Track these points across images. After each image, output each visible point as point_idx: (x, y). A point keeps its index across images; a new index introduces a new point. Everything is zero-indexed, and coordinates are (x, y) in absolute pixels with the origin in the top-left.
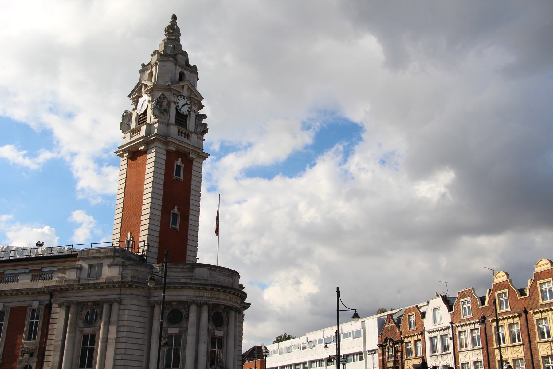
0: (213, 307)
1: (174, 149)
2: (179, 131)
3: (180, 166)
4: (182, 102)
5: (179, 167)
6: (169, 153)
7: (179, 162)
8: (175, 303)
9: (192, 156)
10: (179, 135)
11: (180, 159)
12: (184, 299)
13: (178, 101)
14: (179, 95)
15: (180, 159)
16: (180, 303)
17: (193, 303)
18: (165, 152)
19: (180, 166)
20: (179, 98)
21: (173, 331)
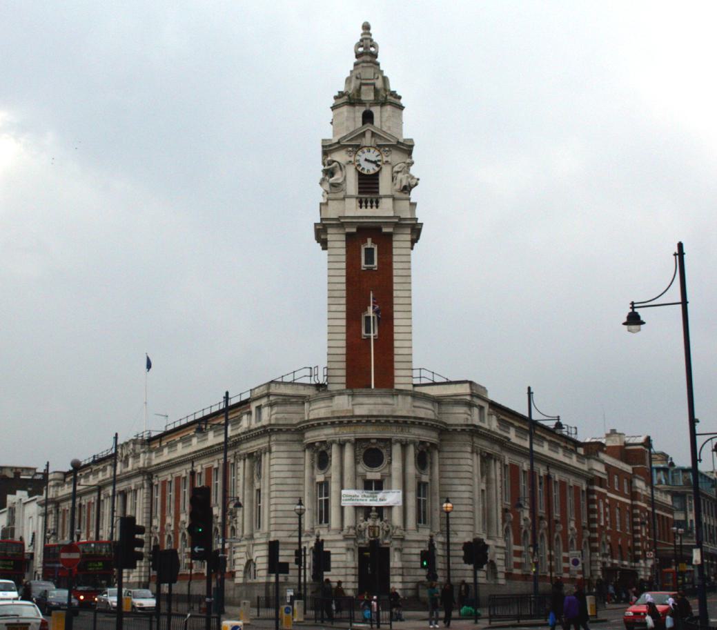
0: (357, 442)
1: (354, 230)
2: (361, 202)
3: (372, 249)
4: (362, 156)
5: (369, 252)
6: (350, 238)
7: (369, 244)
8: (374, 441)
9: (385, 230)
10: (361, 207)
11: (369, 240)
12: (323, 438)
13: (358, 158)
14: (358, 147)
15: (369, 240)
16: (324, 442)
17: (334, 442)
18: (343, 237)
19: (372, 249)
20: (360, 153)
21: (320, 478)
